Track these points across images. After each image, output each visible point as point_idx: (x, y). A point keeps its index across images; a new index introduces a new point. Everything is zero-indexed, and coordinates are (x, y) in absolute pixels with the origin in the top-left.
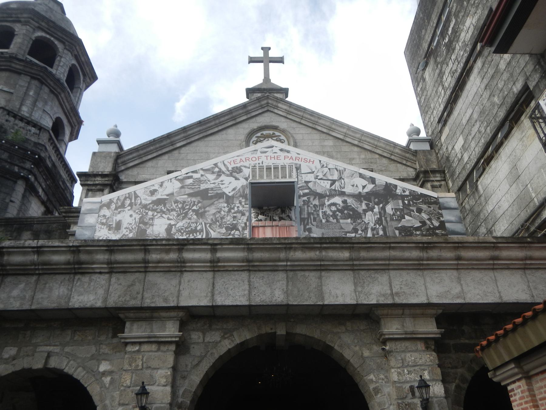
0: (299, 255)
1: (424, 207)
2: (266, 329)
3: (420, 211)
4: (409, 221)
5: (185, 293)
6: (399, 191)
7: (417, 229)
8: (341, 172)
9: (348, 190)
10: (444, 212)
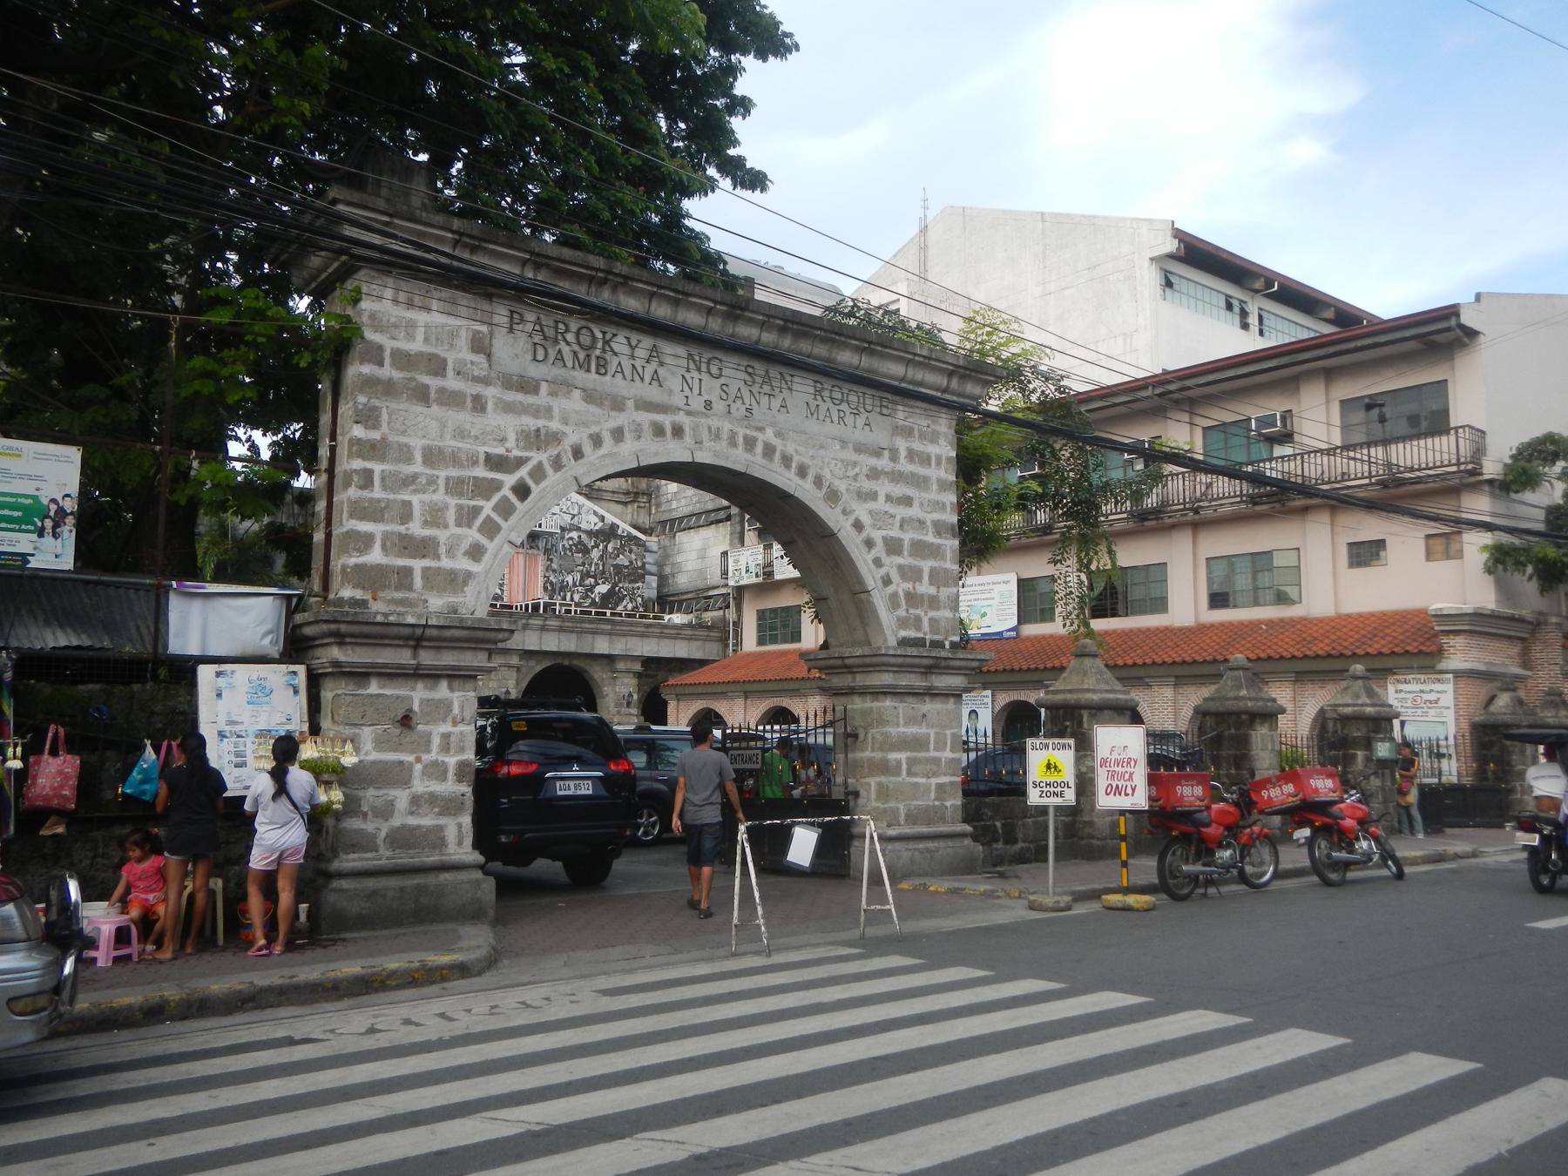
0: (587, 625)
1: (634, 548)
2: (558, 661)
3: (631, 551)
4: (622, 560)
5: (527, 642)
6: (620, 532)
7: (626, 567)
8: (580, 507)
9: (584, 526)
10: (647, 554)
